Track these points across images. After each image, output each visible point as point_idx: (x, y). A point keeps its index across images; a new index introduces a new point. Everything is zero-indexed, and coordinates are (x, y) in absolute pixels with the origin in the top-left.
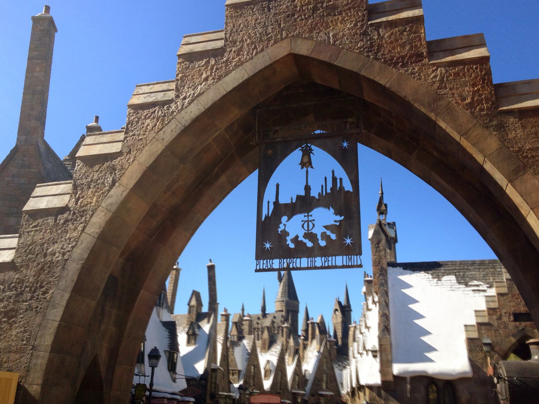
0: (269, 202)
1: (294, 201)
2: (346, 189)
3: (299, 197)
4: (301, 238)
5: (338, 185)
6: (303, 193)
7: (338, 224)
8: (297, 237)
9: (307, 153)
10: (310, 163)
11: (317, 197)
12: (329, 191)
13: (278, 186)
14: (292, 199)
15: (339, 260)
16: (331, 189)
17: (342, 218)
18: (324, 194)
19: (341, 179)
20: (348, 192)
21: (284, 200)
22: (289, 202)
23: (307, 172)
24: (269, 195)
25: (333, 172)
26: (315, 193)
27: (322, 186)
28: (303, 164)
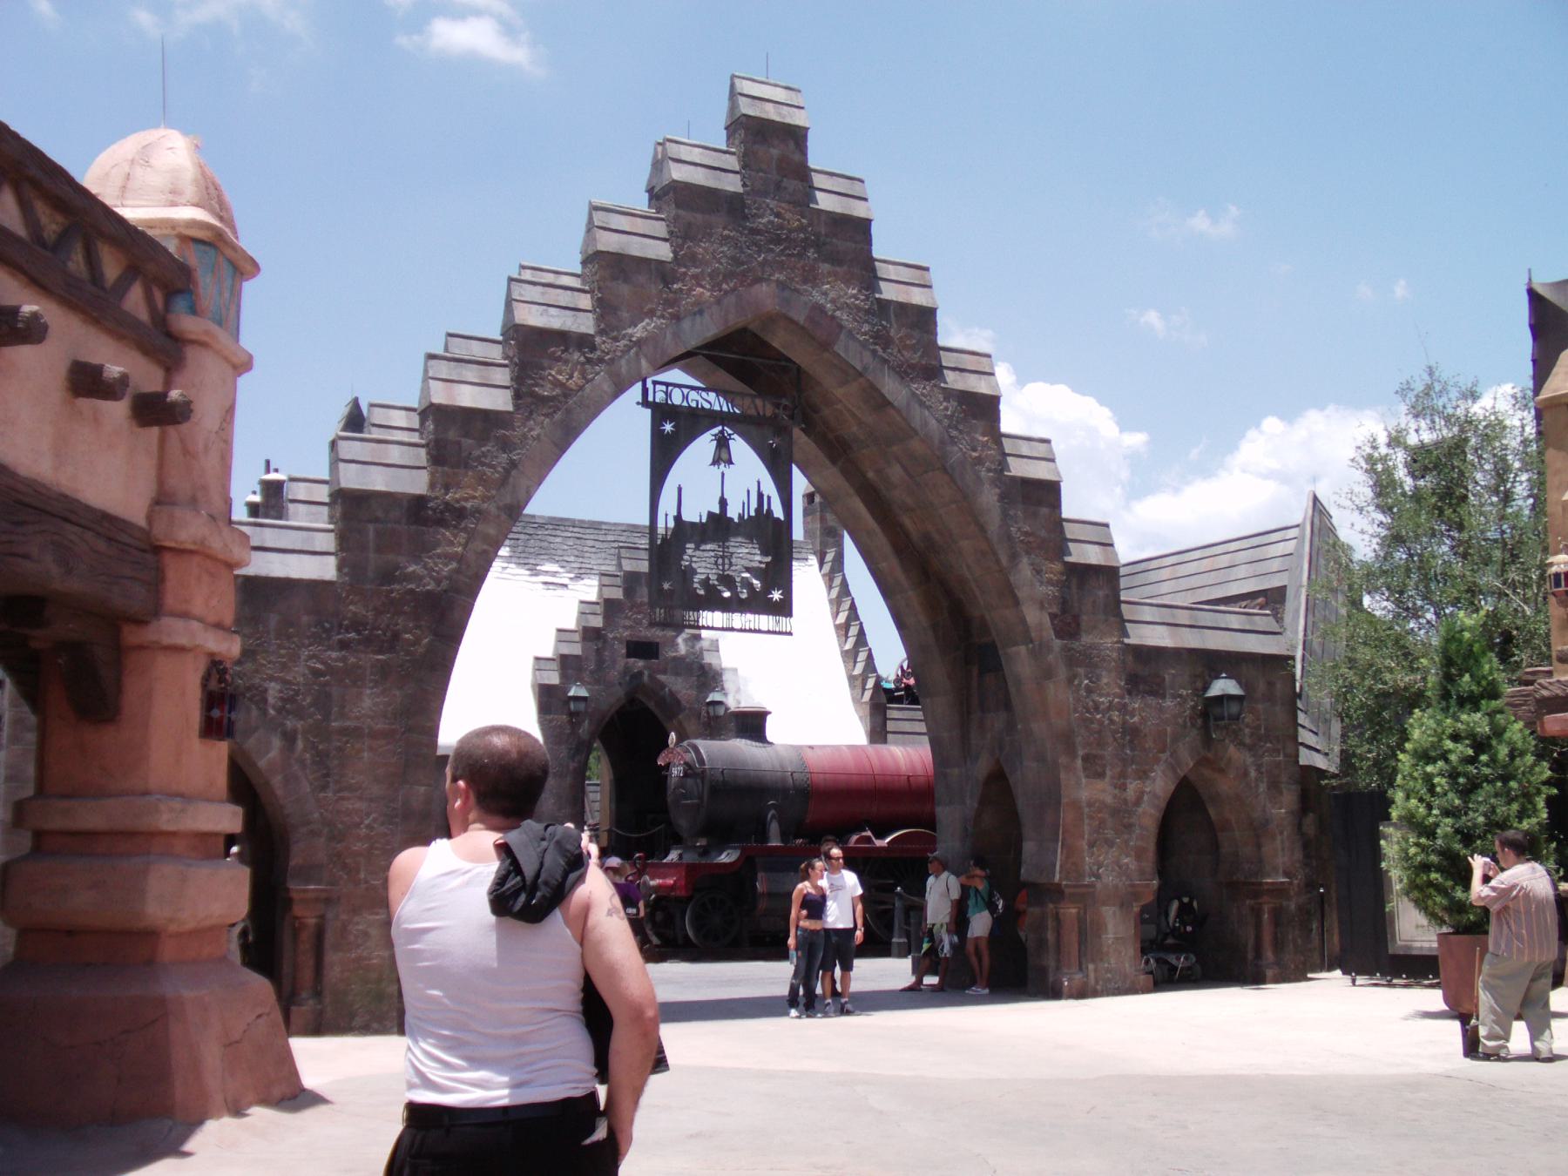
0: (666, 515)
1: (704, 520)
2: (775, 516)
3: (710, 515)
4: (714, 580)
5: (766, 507)
6: (716, 510)
7: (763, 566)
8: (708, 579)
9: (722, 443)
10: (730, 462)
11: (736, 520)
12: (753, 513)
13: (680, 489)
14: (701, 516)
15: (765, 621)
16: (756, 510)
17: (769, 559)
18: (746, 517)
19: (769, 498)
20: (778, 519)
21: (690, 516)
22: (697, 520)
23: (723, 474)
24: (667, 505)
25: (759, 483)
26: (733, 512)
27: (744, 504)
28: (716, 462)
